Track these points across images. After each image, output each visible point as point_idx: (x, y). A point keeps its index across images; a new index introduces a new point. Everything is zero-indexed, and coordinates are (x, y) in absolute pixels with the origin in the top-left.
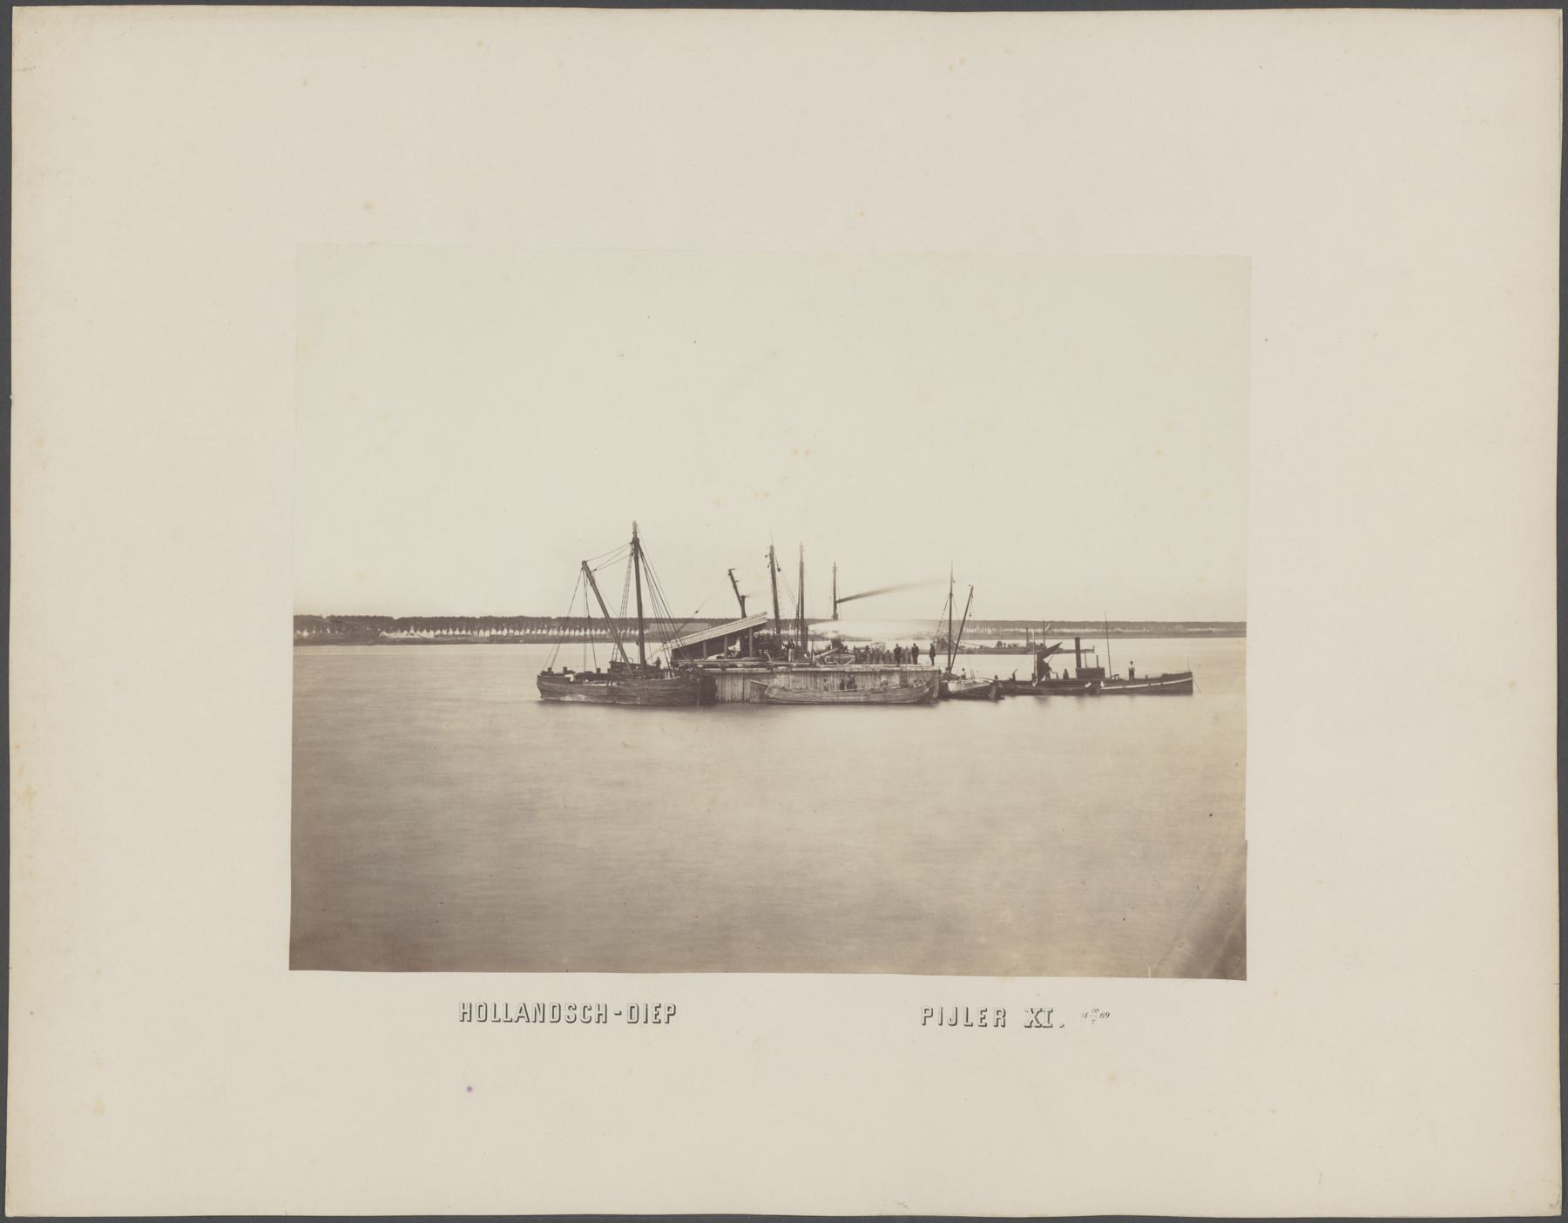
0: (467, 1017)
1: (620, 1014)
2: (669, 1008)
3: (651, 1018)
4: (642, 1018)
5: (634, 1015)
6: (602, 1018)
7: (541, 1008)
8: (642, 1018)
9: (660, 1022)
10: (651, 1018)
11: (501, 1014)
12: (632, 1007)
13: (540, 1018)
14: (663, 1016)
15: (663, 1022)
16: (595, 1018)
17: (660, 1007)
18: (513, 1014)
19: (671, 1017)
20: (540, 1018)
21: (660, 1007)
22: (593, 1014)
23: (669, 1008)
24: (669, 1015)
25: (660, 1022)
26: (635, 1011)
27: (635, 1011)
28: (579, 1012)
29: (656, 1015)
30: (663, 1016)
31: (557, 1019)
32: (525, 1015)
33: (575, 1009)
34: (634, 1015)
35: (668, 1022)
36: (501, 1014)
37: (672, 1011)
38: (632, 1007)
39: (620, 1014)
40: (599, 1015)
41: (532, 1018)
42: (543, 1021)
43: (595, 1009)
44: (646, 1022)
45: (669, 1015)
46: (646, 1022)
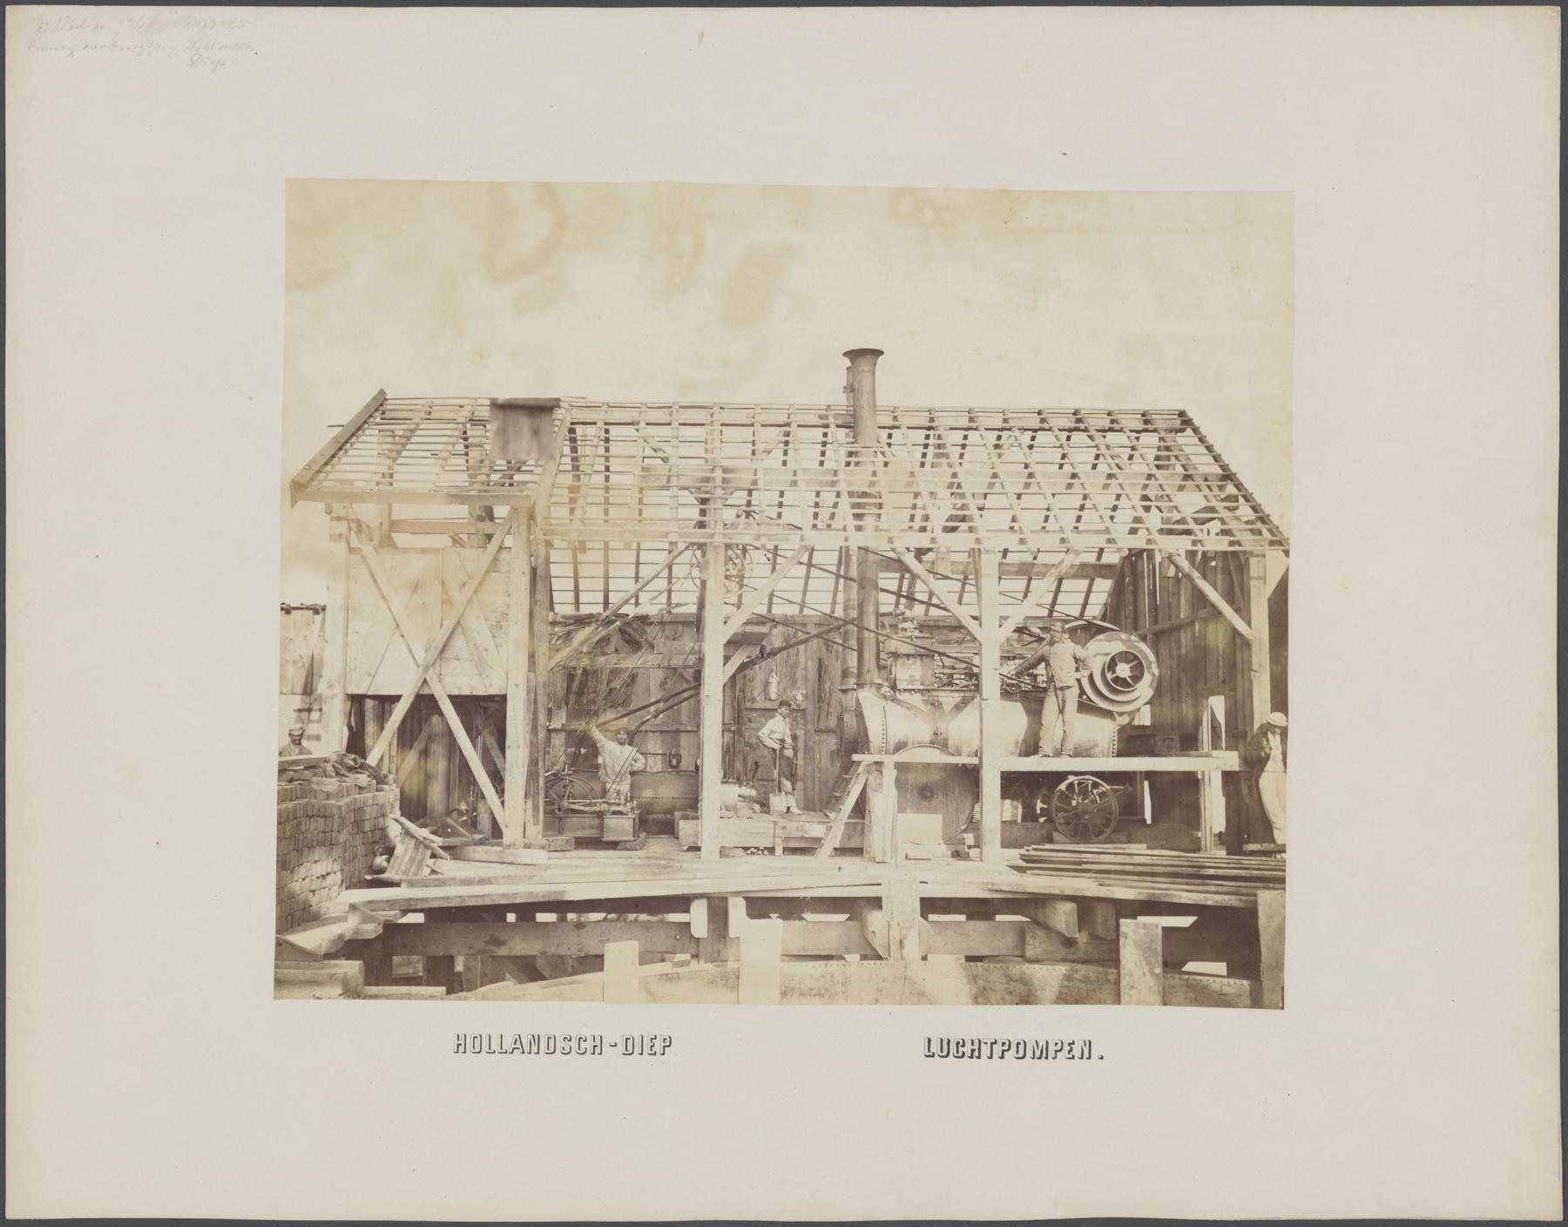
0: (462, 1048)
1: (616, 1045)
2: (665, 1039)
3: (646, 1049)
4: (638, 1050)
5: (629, 1046)
6: (597, 1049)
7: (536, 1039)
8: (638, 1050)
9: (655, 1054)
10: (646, 1049)
11: (495, 1046)
12: (627, 1039)
13: (535, 1049)
14: (658, 1048)
15: (658, 1054)
16: (590, 1050)
17: (655, 1038)
18: (508, 1045)
19: (666, 1049)
20: (535, 1049)
21: (655, 1038)
22: (589, 1045)
23: (665, 1039)
24: (664, 1047)
25: (655, 1054)
26: (630, 1042)
27: (630, 1042)
28: (574, 1044)
29: (652, 1046)
30: (658, 1048)
31: (552, 1051)
32: (518, 1045)
33: (570, 1040)
34: (629, 1046)
35: (663, 1054)
36: (495, 1046)
37: (668, 1044)
38: (627, 1039)
39: (616, 1045)
40: (595, 1046)
41: (527, 1049)
42: (538, 1053)
43: (590, 1039)
44: (642, 1054)
45: (664, 1047)
46: (642, 1054)
